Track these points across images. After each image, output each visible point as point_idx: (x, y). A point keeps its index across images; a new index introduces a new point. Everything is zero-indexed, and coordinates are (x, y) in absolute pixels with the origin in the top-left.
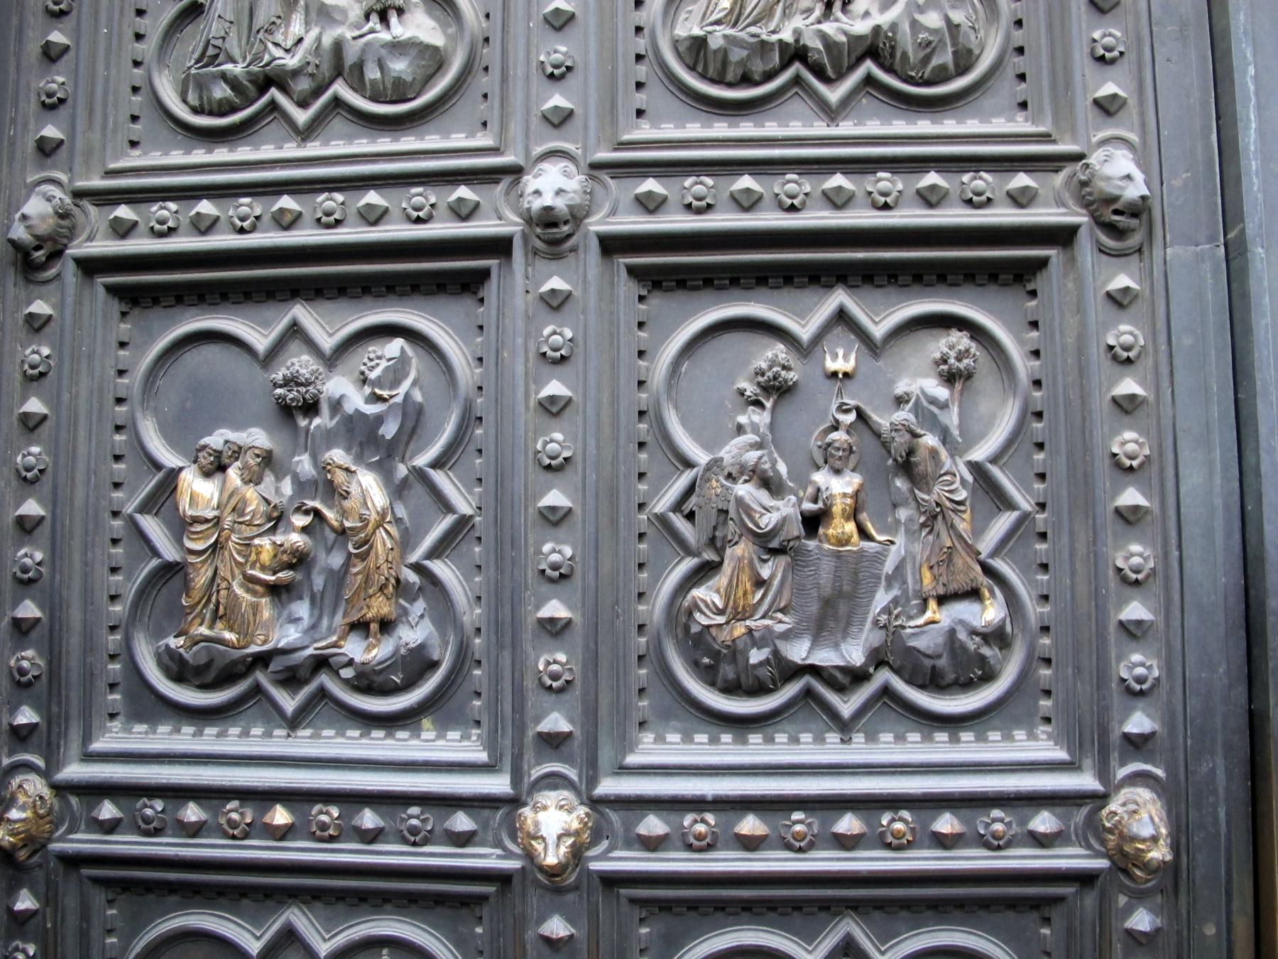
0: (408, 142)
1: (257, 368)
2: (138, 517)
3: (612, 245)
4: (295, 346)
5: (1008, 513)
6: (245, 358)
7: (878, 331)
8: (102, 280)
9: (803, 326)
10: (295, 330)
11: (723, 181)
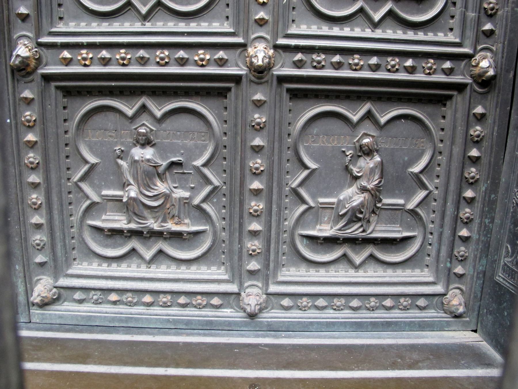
0: (193, 26)
1: (127, 123)
2: (79, 184)
3: (282, 80)
4: (145, 116)
5: (424, 191)
6: (123, 120)
7: (383, 120)
8: (53, 84)
9: (355, 115)
10: (144, 108)
11: (329, 56)
